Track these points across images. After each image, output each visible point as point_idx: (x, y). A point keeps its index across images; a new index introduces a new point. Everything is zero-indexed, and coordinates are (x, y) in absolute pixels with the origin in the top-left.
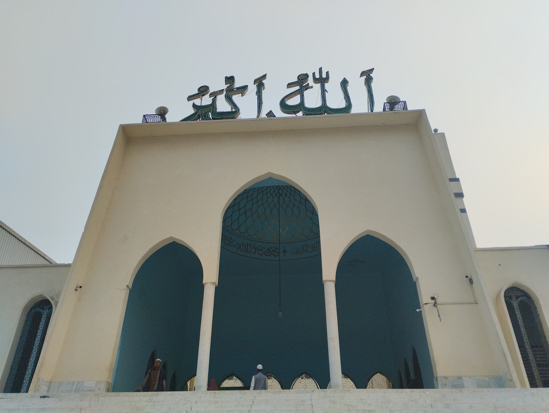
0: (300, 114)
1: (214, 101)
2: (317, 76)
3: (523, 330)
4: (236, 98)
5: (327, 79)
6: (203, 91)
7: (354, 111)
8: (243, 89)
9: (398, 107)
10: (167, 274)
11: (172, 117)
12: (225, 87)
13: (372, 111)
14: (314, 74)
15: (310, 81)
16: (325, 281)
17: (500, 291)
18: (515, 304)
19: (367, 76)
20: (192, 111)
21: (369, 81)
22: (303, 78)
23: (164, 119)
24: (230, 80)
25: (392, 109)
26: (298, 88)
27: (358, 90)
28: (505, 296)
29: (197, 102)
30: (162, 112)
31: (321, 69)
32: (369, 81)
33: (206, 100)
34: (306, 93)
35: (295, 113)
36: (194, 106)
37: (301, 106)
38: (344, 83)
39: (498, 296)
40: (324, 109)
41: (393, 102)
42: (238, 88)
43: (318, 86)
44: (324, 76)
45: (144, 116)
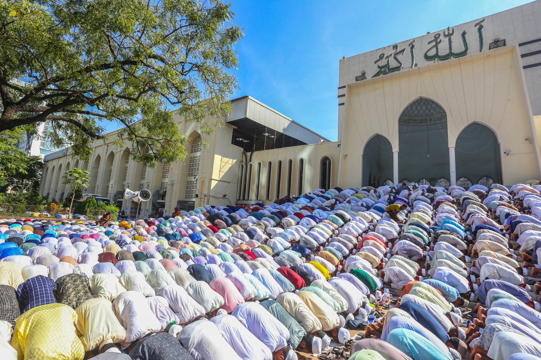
1: (388, 62)
4: (399, 57)
11: (369, 76)
12: (393, 52)
14: (444, 32)
15: (442, 37)
26: (434, 44)
29: (380, 64)
30: (364, 74)
33: (383, 62)
34: (440, 46)
36: (379, 67)
37: (436, 56)
38: (464, 34)
40: (451, 54)
42: (400, 52)
44: (451, 32)
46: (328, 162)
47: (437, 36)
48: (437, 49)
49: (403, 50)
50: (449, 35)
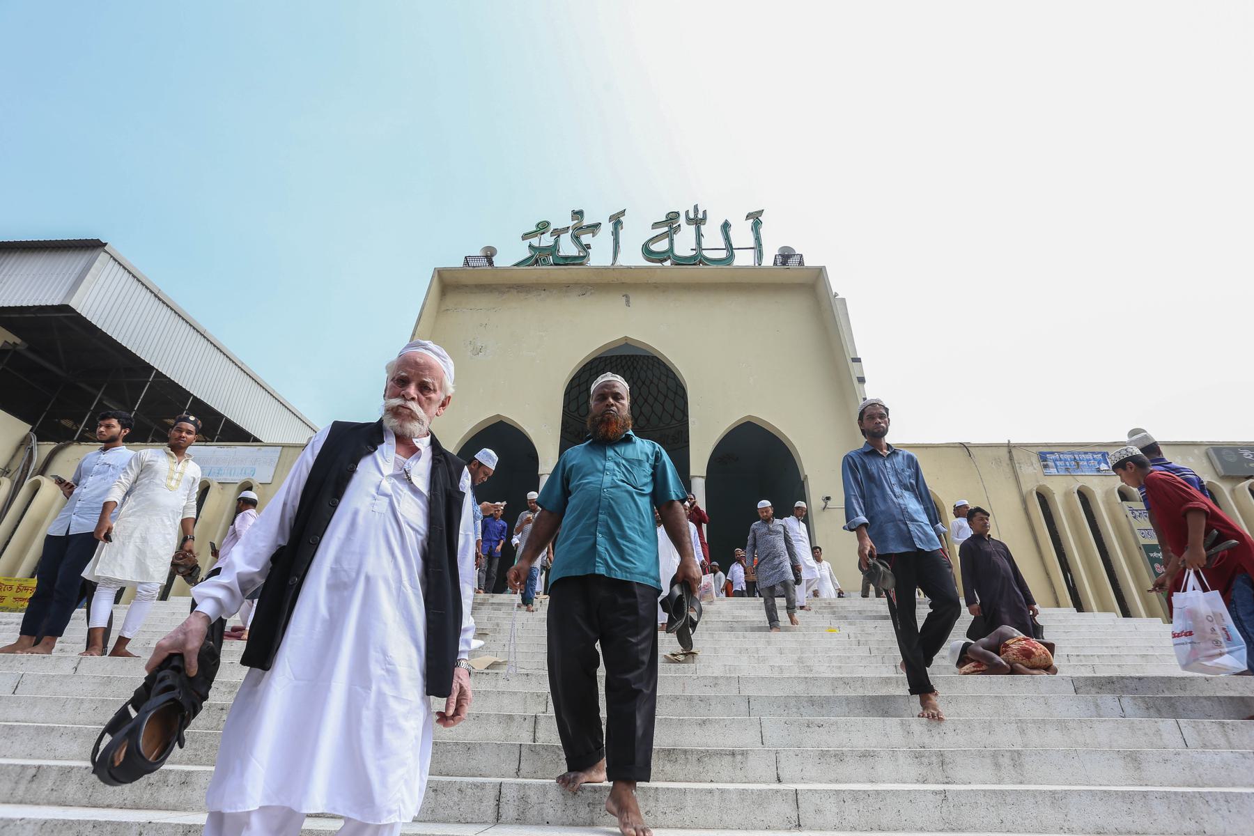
0: (668, 263)
1: (556, 242)
2: (692, 216)
4: (586, 239)
5: (704, 219)
6: (543, 227)
8: (594, 228)
9: (793, 262)
12: (571, 223)
14: (687, 212)
15: (682, 220)
19: (755, 218)
21: (757, 225)
22: (672, 218)
23: (491, 263)
24: (578, 214)
25: (784, 263)
26: (666, 229)
27: (742, 235)
29: (535, 242)
30: (489, 255)
31: (696, 208)
32: (757, 225)
33: (547, 240)
35: (661, 261)
36: (530, 246)
37: (668, 254)
38: (726, 226)
40: (697, 259)
42: (588, 227)
43: (693, 228)
44: (700, 216)
49: (597, 225)
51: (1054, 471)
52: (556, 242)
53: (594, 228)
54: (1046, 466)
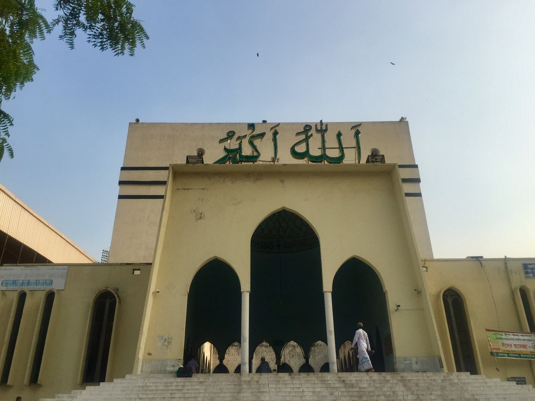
1: (240, 144)
3: (453, 319)
4: (257, 142)
5: (326, 130)
6: (231, 135)
7: (345, 161)
8: (262, 135)
10: (213, 280)
11: (209, 159)
13: (359, 163)
15: (313, 131)
16: (325, 292)
17: (441, 291)
18: (450, 302)
20: (223, 154)
26: (303, 137)
27: (348, 140)
28: (443, 295)
30: (201, 153)
32: (357, 133)
36: (225, 149)
38: (339, 135)
39: (438, 296)
40: (323, 157)
41: (375, 157)
44: (324, 128)
45: (187, 157)
46: (108, 302)
47: (307, 128)
48: (308, 145)
50: (323, 129)
51: (531, 275)
52: (240, 144)
53: (262, 135)
54: (527, 273)
